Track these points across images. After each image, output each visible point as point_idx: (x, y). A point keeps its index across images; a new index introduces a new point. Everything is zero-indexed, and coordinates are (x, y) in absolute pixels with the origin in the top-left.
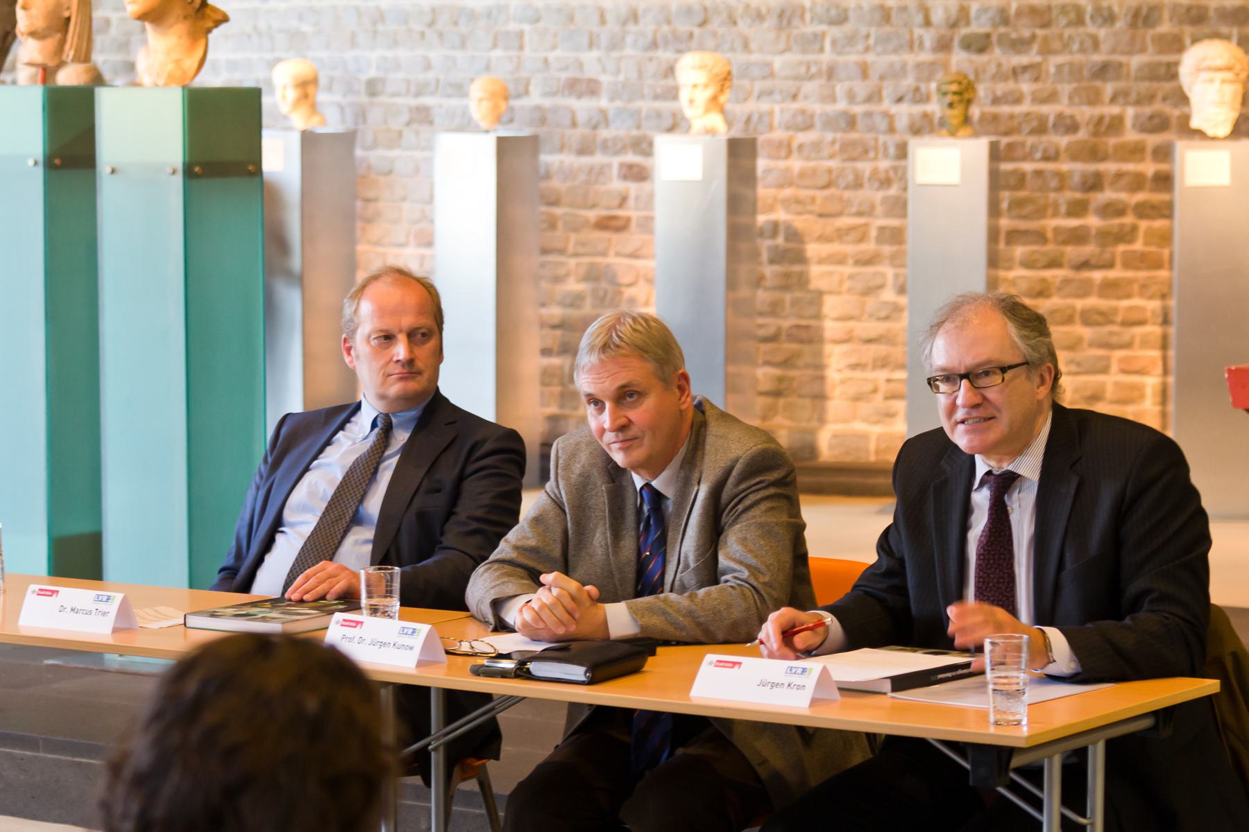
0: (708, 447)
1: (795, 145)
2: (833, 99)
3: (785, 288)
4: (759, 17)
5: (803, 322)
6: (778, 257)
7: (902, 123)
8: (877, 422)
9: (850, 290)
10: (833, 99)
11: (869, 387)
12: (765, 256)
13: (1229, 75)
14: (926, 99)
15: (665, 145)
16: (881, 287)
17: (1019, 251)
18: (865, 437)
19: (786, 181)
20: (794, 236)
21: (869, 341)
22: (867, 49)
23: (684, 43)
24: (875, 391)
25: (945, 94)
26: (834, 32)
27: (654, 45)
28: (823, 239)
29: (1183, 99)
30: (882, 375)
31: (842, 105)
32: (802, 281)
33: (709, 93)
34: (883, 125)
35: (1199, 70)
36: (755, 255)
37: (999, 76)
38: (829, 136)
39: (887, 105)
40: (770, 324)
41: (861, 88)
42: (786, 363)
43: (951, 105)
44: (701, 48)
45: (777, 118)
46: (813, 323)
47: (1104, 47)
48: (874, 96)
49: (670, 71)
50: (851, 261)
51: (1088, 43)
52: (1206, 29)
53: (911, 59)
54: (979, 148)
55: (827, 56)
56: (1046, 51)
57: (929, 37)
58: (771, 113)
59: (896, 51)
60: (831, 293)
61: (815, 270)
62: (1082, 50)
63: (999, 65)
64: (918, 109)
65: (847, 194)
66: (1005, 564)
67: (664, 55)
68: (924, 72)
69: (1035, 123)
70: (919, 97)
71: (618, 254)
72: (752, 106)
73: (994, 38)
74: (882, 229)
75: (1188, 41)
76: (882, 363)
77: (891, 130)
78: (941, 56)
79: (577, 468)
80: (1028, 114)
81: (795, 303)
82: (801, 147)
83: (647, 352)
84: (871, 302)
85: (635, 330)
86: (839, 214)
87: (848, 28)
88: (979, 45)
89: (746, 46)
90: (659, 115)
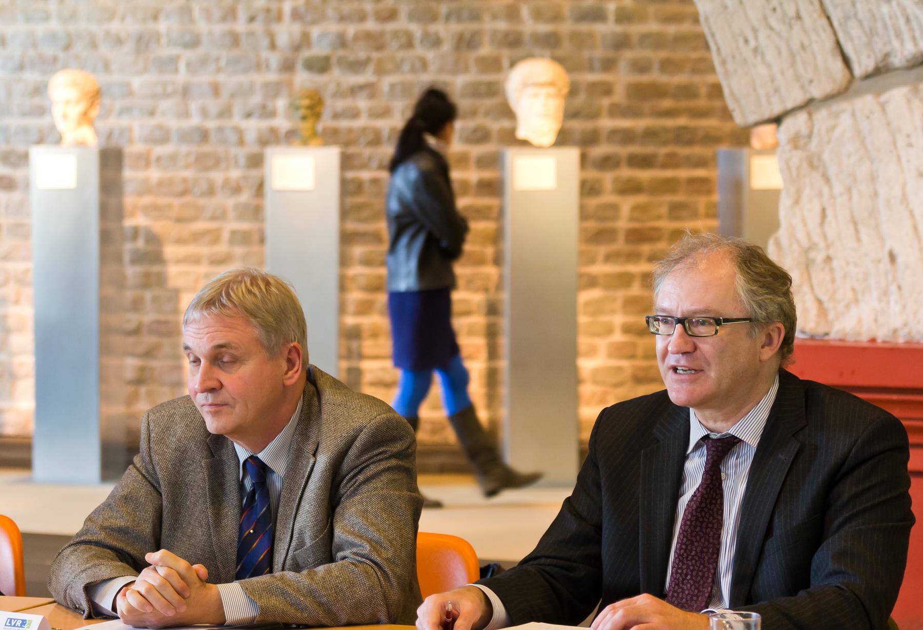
0: (324, 416)
1: (153, 156)
2: (186, 114)
4: (119, 41)
5: (162, 317)
6: (139, 258)
7: (251, 137)
10: (186, 114)
12: (127, 257)
13: (551, 90)
14: (272, 114)
15: (40, 156)
17: (358, 251)
19: (146, 189)
20: (153, 239)
22: (219, 70)
23: (51, 65)
25: (297, 108)
26: (188, 55)
27: (21, 67)
28: (180, 241)
29: (508, 113)
31: (195, 121)
32: (160, 280)
33: (80, 108)
34: (232, 137)
35: (525, 85)
36: (119, 259)
37: (339, 94)
38: (184, 149)
39: (237, 120)
40: (132, 319)
41: (214, 105)
42: (149, 354)
43: (304, 118)
44: (65, 67)
45: (137, 133)
46: (171, 318)
47: (432, 67)
48: (225, 113)
49: (40, 90)
51: (418, 65)
52: (519, 52)
53: (259, 78)
54: (331, 155)
55: (182, 76)
56: (380, 71)
57: (274, 59)
58: (130, 129)
59: (245, 71)
62: (413, 70)
63: (338, 85)
64: (265, 124)
65: (202, 201)
66: (711, 534)
67: (32, 77)
68: (273, 90)
69: (371, 136)
70: (267, 112)
72: (115, 122)
73: (334, 60)
74: (234, 233)
75: (506, 63)
77: (241, 142)
78: (285, 76)
79: (172, 442)
80: (364, 130)
81: (155, 299)
82: (159, 159)
83: (255, 316)
85: (250, 292)
86: (194, 219)
87: (200, 51)
88: (320, 66)
89: (107, 67)
90: (26, 131)
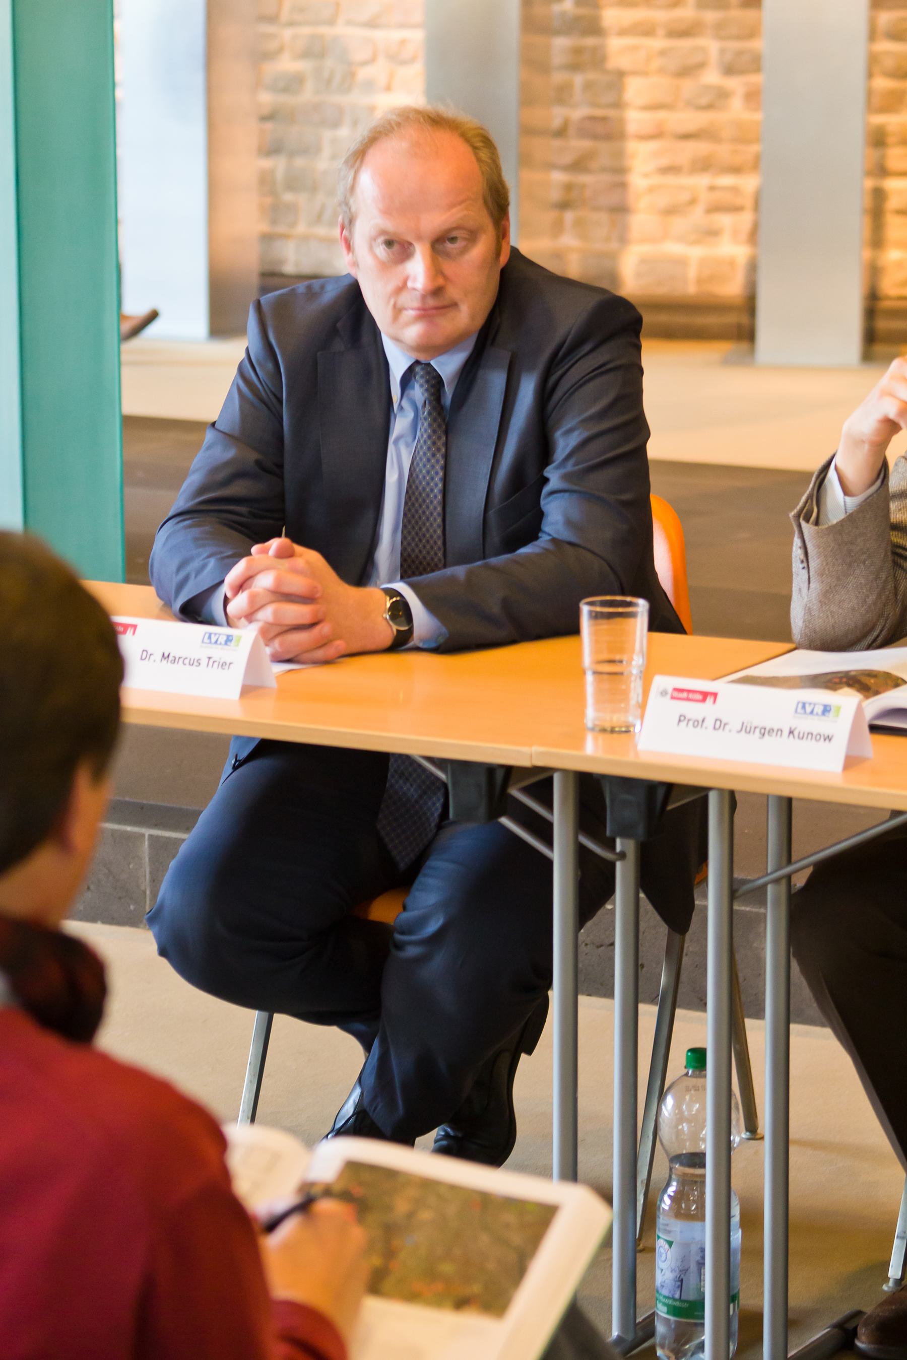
3: (575, 67)
5: (599, 112)
8: (696, 242)
9: (661, 71)
11: (685, 197)
16: (701, 66)
18: (682, 262)
21: (687, 136)
24: (693, 201)
30: (703, 181)
32: (598, 59)
40: (558, 115)
42: (578, 165)
46: (611, 113)
50: (661, 32)
60: (635, 73)
61: (614, 44)
71: (349, 23)
76: (704, 165)
81: (588, 86)
84: (688, 86)
